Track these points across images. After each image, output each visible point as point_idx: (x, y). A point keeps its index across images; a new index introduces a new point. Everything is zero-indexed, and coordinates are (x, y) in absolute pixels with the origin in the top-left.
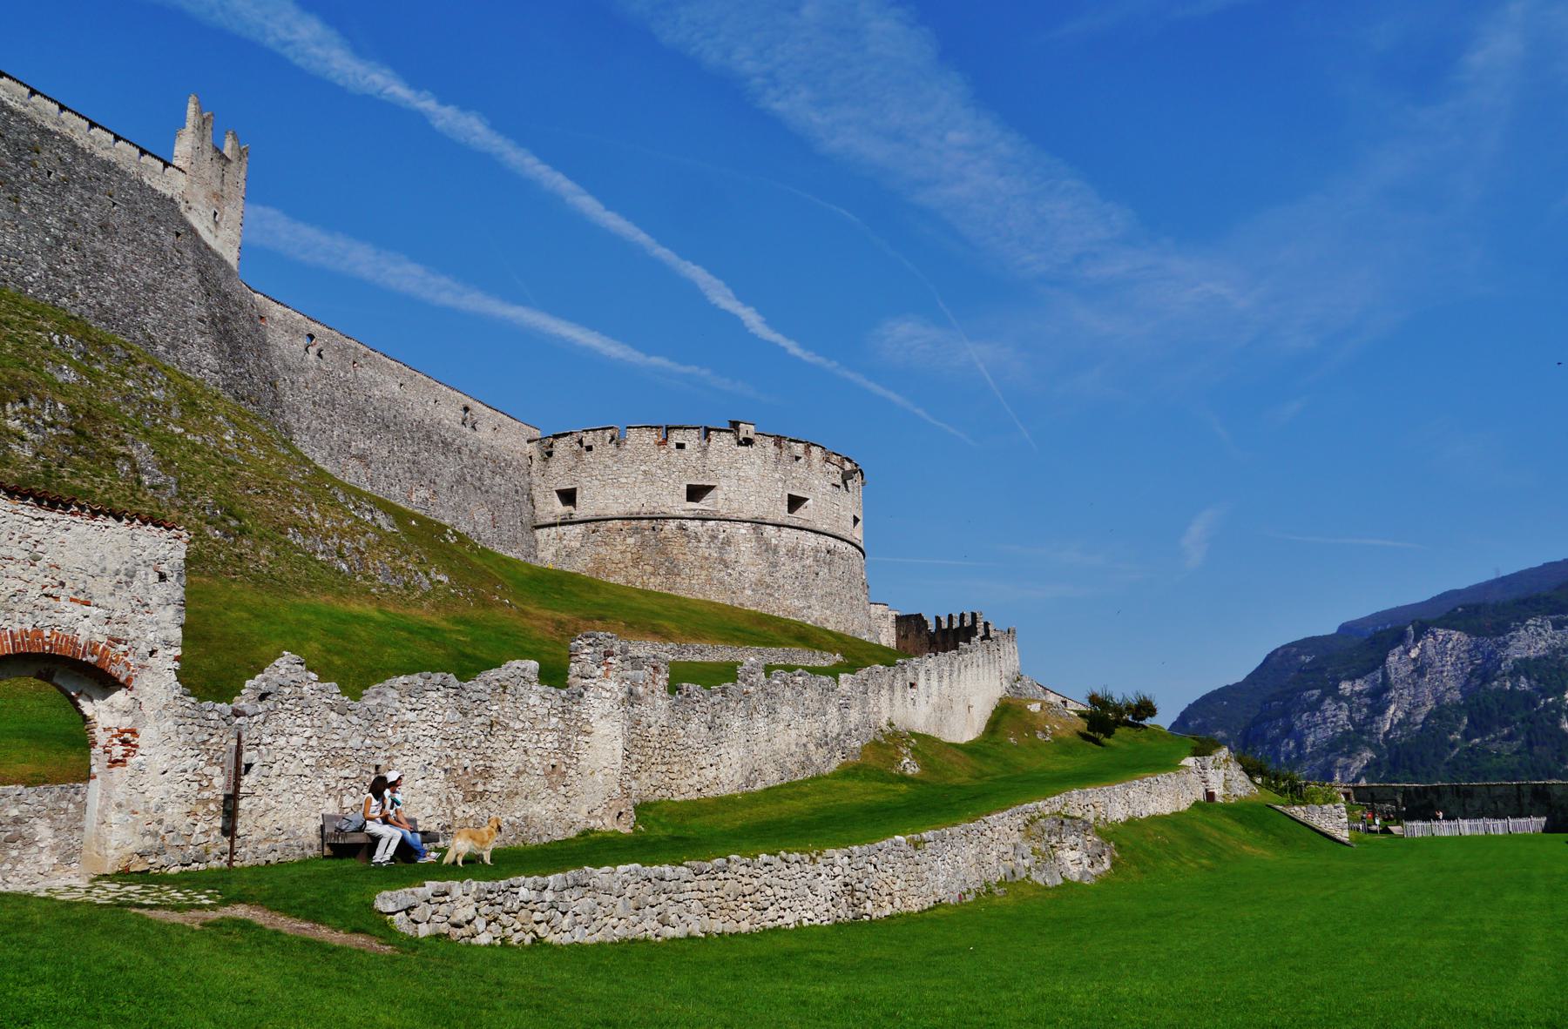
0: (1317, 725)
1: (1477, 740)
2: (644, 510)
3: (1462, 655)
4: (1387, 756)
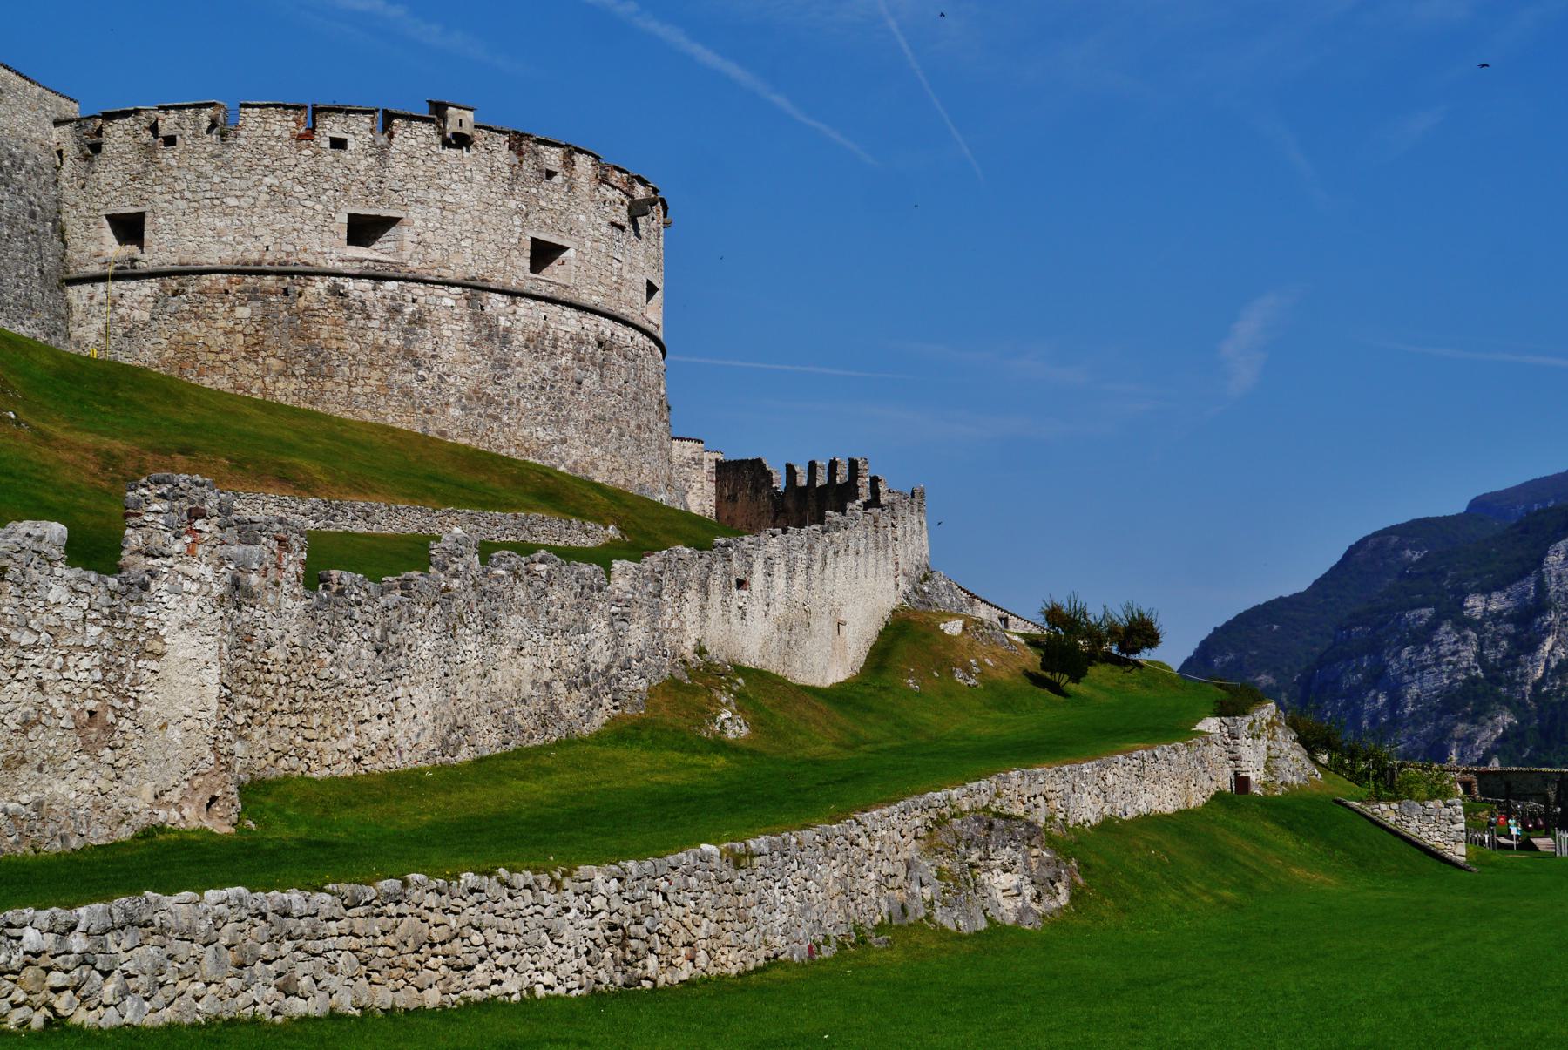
0: (1423, 668)
2: (269, 257)
4: (1537, 721)
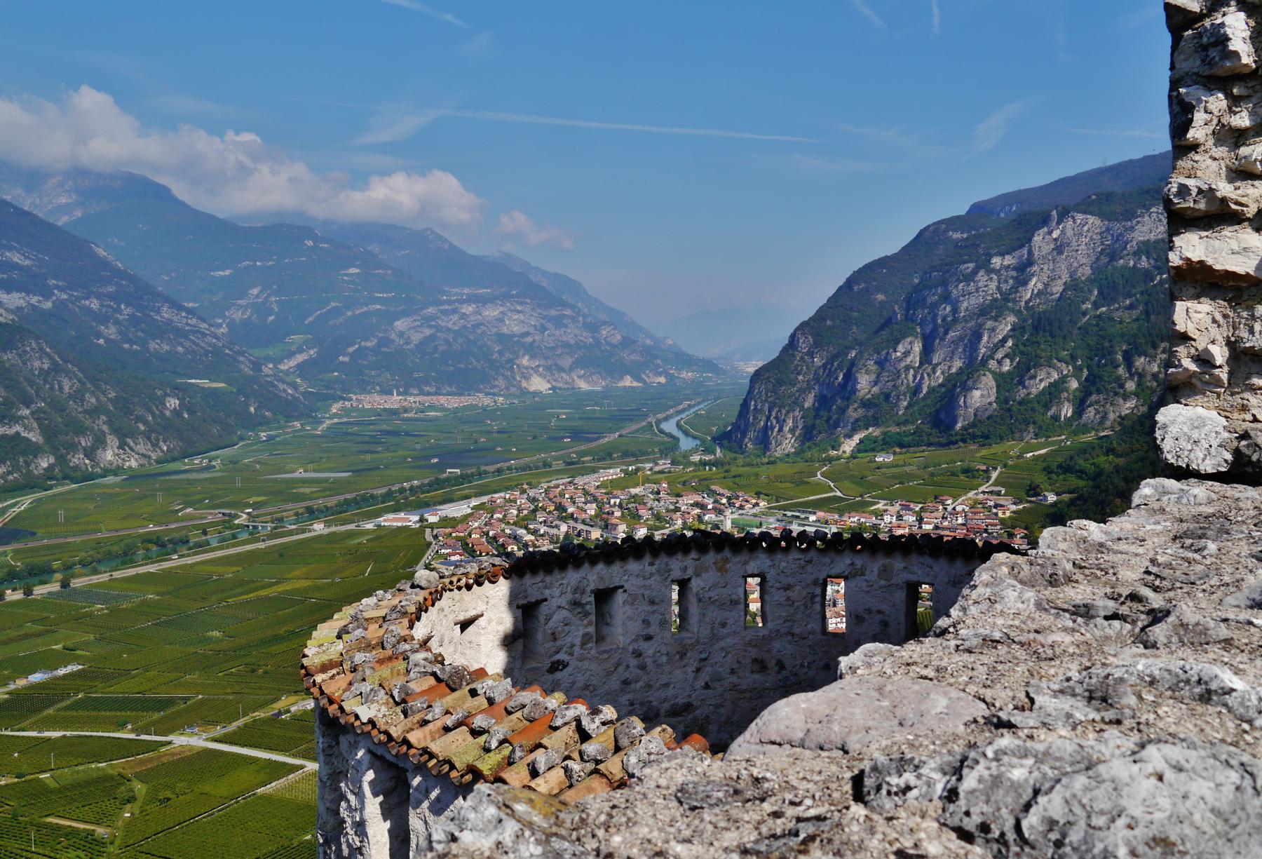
1: (1104, 309)
3: (1094, 237)
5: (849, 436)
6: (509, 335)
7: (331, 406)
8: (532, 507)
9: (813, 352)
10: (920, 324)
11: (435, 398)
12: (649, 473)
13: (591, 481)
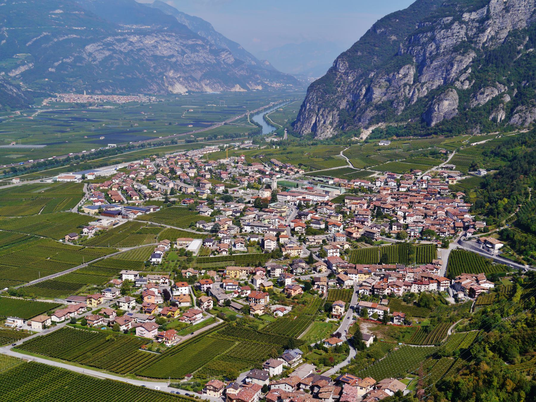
1: (531, 50)
5: (366, 128)
6: (160, 57)
7: (43, 100)
8: (156, 170)
9: (348, 72)
10: (415, 56)
11: (111, 97)
12: (236, 149)
13: (196, 154)
